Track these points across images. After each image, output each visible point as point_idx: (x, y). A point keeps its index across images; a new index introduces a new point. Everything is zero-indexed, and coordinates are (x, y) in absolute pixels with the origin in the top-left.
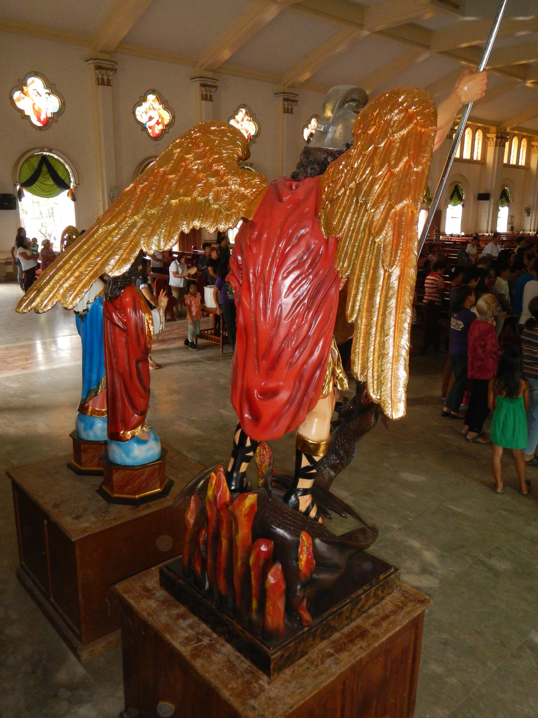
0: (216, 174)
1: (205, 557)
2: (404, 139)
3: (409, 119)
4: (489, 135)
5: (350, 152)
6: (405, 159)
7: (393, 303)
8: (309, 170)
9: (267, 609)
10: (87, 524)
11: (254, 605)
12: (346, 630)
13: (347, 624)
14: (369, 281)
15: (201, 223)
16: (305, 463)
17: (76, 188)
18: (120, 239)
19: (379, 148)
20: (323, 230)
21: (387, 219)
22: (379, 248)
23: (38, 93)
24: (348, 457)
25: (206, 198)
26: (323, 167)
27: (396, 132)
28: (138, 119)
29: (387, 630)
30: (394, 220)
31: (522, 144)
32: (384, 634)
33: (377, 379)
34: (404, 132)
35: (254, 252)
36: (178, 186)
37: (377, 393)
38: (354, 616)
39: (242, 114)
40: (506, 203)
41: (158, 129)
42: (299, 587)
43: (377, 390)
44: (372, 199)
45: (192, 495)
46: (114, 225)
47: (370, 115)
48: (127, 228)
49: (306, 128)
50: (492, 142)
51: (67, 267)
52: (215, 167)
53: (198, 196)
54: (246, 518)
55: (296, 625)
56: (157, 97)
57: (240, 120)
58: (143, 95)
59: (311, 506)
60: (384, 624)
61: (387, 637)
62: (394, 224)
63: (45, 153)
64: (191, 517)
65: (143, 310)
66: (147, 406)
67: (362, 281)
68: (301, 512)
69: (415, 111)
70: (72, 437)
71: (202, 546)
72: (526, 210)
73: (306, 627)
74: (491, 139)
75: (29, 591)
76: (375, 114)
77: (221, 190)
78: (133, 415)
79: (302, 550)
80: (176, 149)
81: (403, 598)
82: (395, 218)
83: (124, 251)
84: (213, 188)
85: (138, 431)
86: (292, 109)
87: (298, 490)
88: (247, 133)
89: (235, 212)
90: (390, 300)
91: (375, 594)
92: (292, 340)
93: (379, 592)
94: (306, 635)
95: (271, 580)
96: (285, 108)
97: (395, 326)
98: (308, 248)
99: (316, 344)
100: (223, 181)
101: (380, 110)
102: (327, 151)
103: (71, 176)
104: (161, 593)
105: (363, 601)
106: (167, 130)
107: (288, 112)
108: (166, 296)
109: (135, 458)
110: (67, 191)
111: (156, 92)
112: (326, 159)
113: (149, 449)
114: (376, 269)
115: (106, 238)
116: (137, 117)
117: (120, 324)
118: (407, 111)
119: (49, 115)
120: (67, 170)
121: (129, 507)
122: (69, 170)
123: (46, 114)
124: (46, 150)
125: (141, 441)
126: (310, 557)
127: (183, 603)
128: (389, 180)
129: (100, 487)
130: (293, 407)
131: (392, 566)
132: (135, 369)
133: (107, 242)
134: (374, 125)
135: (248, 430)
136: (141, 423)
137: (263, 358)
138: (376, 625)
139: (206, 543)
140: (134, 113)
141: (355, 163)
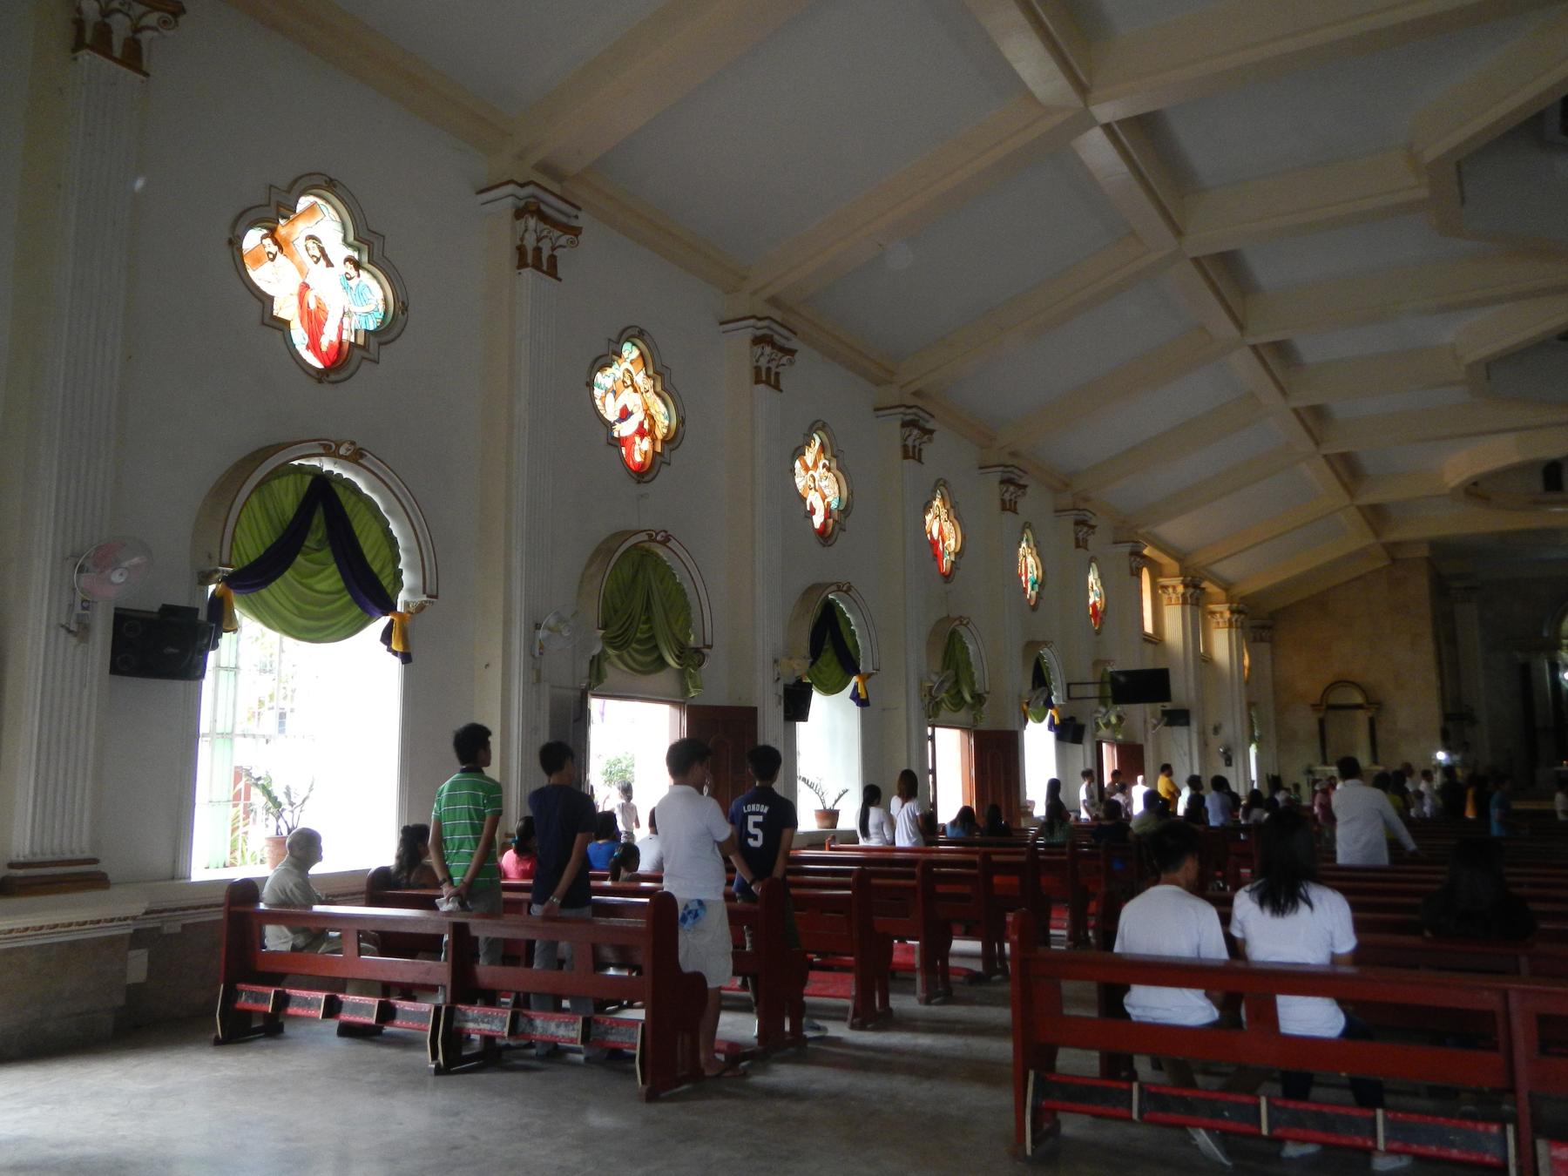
4: (1163, 581)
41: (641, 450)
50: (1174, 596)
56: (642, 355)
58: (614, 337)
63: (327, 466)
74: (1171, 590)
88: (824, 501)
106: (667, 453)
119: (348, 337)
120: (393, 542)
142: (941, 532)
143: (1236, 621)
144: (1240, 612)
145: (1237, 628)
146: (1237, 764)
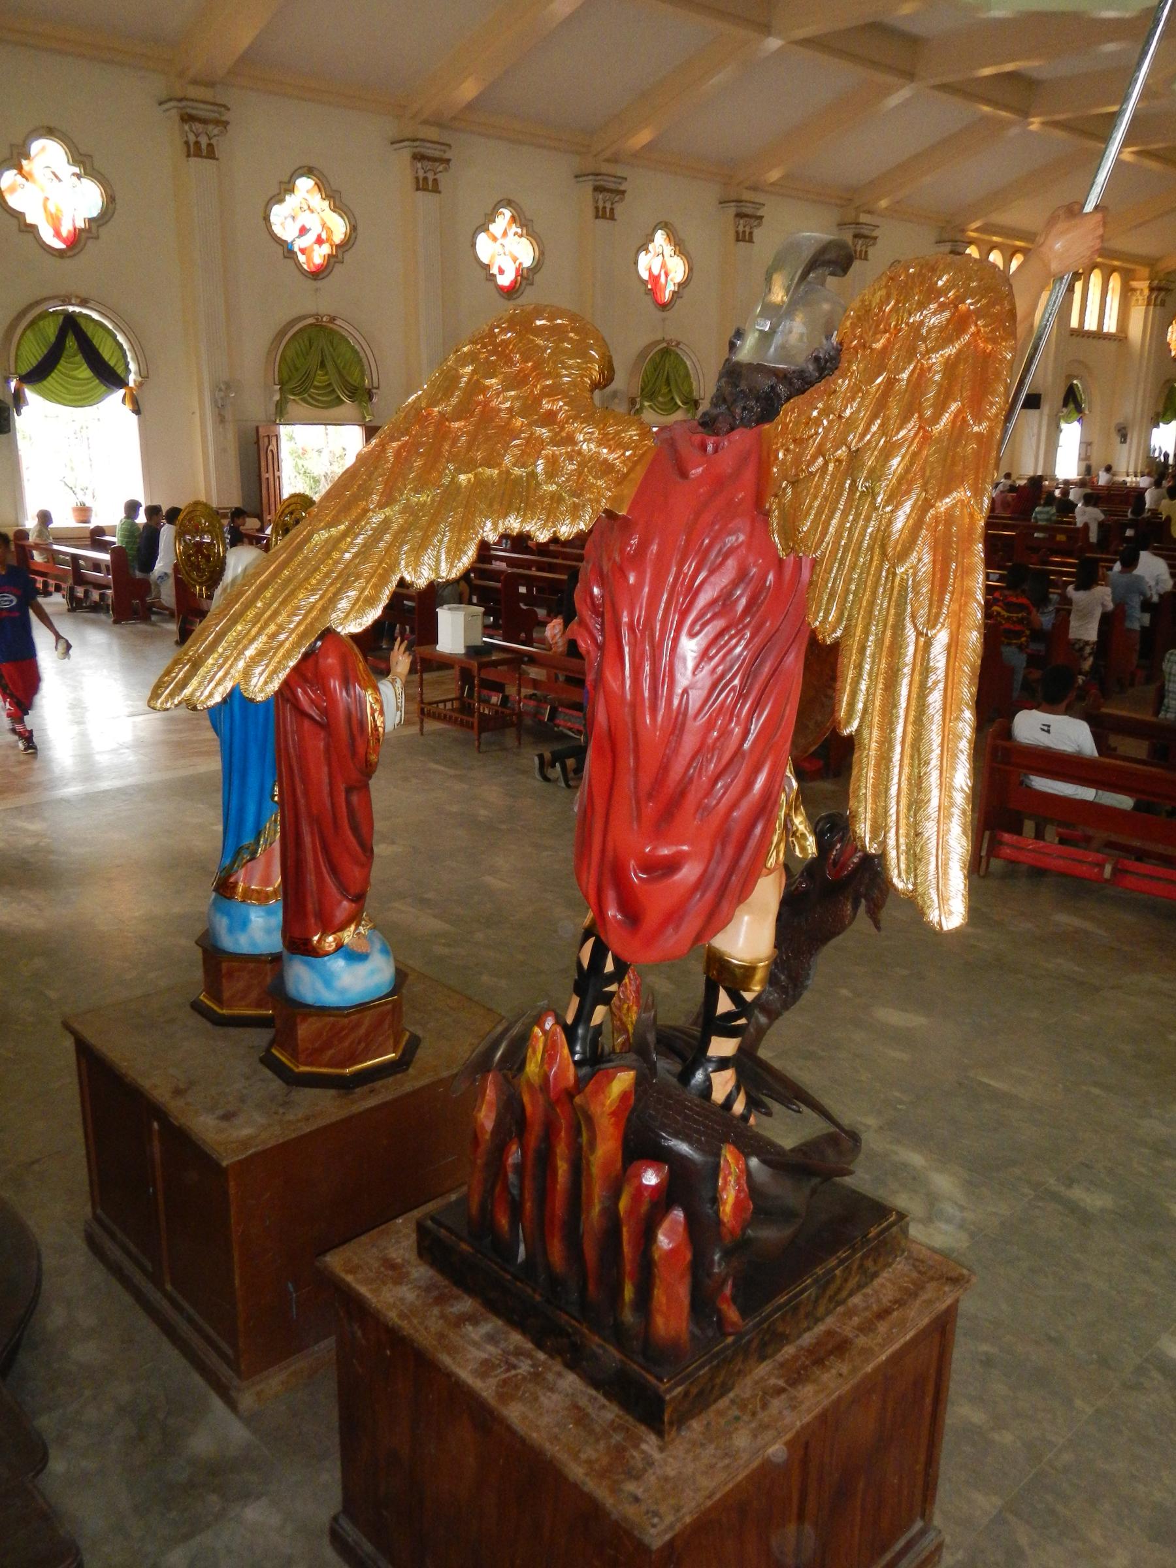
0: (549, 419)
1: (517, 1198)
2: (950, 366)
3: (959, 324)
5: (836, 384)
6: (954, 407)
7: (935, 699)
8: (738, 411)
9: (655, 1304)
10: (246, 1132)
11: (629, 1293)
12: (807, 1339)
13: (809, 1329)
14: (884, 654)
15: (522, 522)
16: (724, 1004)
17: (140, 385)
18: (356, 556)
19: (899, 380)
20: (777, 539)
21: (921, 528)
22: (904, 588)
23: (54, 174)
24: (796, 986)
25: (530, 469)
26: (769, 409)
27: (935, 350)
28: (276, 232)
29: (889, 1340)
30: (935, 531)
31: (1111, 286)
32: (882, 1346)
33: (907, 853)
34: (950, 351)
35: (632, 580)
36: (470, 445)
37: (908, 879)
38: (821, 1310)
39: (503, 220)
40: (1076, 415)
41: (319, 255)
42: (716, 1257)
43: (908, 873)
44: (887, 486)
45: (489, 1071)
46: (342, 527)
47: (876, 311)
48: (369, 533)
49: (644, 252)
51: (250, 614)
52: (546, 405)
53: (514, 465)
54: (613, 1119)
55: (710, 1333)
56: (316, 184)
57: (498, 234)
58: (286, 179)
59: (735, 1093)
60: (882, 1327)
61: (889, 1351)
62: (936, 541)
63: (71, 309)
64: (486, 1116)
65: (362, 683)
66: (366, 881)
67: (868, 652)
68: (715, 1104)
69: (972, 307)
70: (200, 946)
71: (512, 1177)
72: (1119, 431)
73: (730, 1334)
75: (116, 1270)
76: (888, 309)
77: (561, 455)
78: (340, 903)
79: (726, 1182)
80: (464, 366)
81: (915, 1275)
82: (936, 527)
83: (367, 583)
84: (543, 449)
85: (348, 935)
86: (612, 210)
87: (709, 1060)
89: (590, 500)
90: (930, 693)
91: (861, 1266)
92: (709, 761)
93: (869, 1263)
94: (729, 1352)
95: (664, 1241)
96: (597, 208)
97: (942, 745)
98: (742, 575)
99: (756, 770)
100: (564, 434)
101: (897, 302)
102: (774, 372)
103: (129, 359)
104: (421, 1272)
105: (838, 1282)
106: (340, 256)
107: (604, 217)
108: (407, 653)
109: (342, 992)
110: (122, 392)
111: (315, 172)
112: (773, 388)
113: (372, 972)
114: (899, 628)
115: (328, 555)
116: (273, 227)
117: (314, 712)
118: (956, 307)
119: (81, 224)
120: (120, 346)
121: (332, 1092)
122: (126, 346)
123: (74, 221)
124: (73, 302)
125: (355, 956)
126: (742, 1195)
127: (471, 1291)
128: (920, 449)
129: (268, 1051)
130: (710, 894)
131: (894, 1210)
132: (344, 804)
133: (330, 562)
134: (886, 331)
135: (615, 939)
136: (354, 918)
137: (650, 797)
138: (867, 1328)
139: (520, 1169)
140: (267, 218)
141: (846, 408)
142: (663, 265)
143: (1156, 298)
144: (1159, 289)
145: (1155, 305)
146: (1131, 444)
